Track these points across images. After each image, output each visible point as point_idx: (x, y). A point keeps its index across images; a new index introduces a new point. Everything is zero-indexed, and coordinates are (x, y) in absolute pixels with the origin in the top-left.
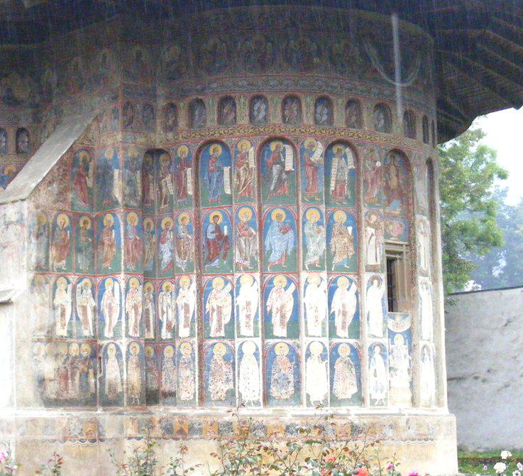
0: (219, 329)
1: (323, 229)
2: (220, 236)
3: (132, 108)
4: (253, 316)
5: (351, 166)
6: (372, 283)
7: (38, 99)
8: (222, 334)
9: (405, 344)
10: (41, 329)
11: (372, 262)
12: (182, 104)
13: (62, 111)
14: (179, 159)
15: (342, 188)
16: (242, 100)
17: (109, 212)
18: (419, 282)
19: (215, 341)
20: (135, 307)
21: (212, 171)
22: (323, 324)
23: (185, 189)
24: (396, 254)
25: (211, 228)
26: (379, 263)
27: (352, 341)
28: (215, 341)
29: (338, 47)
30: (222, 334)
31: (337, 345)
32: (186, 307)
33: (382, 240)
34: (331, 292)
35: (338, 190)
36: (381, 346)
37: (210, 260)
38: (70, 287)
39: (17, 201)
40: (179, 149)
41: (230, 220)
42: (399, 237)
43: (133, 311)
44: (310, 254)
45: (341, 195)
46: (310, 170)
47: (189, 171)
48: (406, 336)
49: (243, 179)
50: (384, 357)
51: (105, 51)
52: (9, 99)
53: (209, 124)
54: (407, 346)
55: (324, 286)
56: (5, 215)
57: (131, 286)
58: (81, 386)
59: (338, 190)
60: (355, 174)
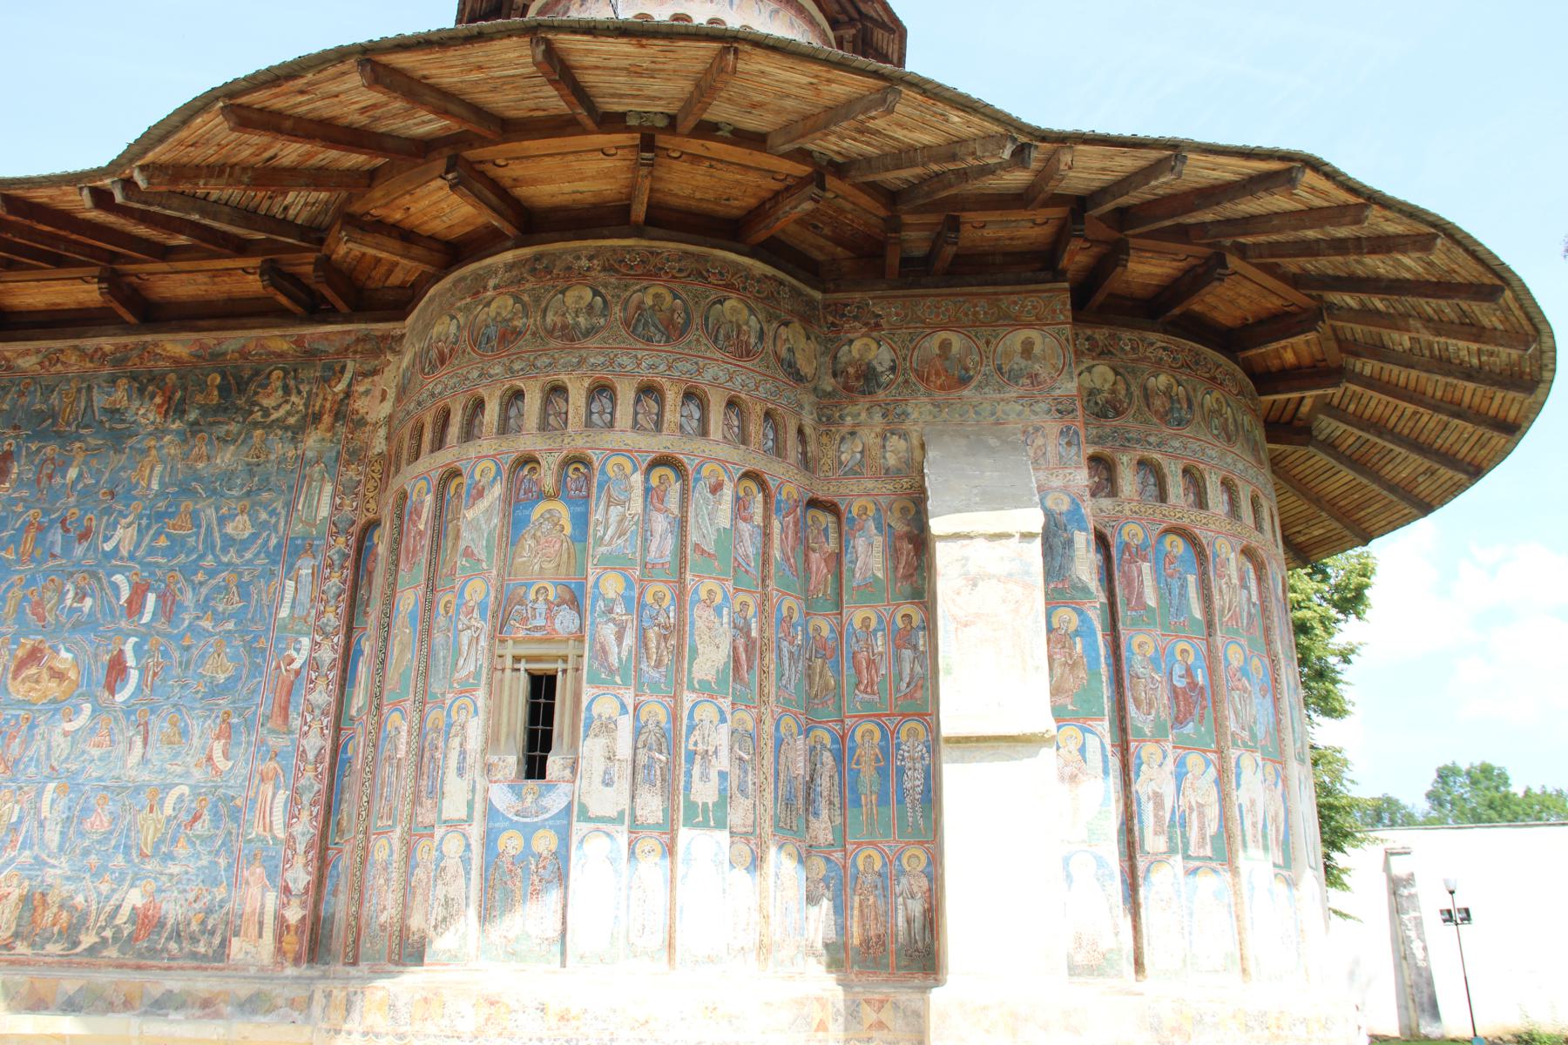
0: (1202, 845)
2: (1193, 685)
4: (1260, 826)
7: (828, 384)
8: (1208, 852)
12: (1125, 459)
13: (905, 414)
14: (1127, 545)
16: (1214, 477)
17: (1066, 605)
19: (1197, 863)
21: (1171, 576)
23: (1140, 595)
25: (1178, 670)
28: (1197, 863)
30: (1208, 852)
32: (1158, 798)
37: (1179, 721)
39: (1008, 536)
40: (1126, 529)
41: (1212, 661)
47: (1146, 567)
49: (1227, 599)
51: (1033, 334)
52: (790, 365)
53: (1172, 499)
56: (967, 559)
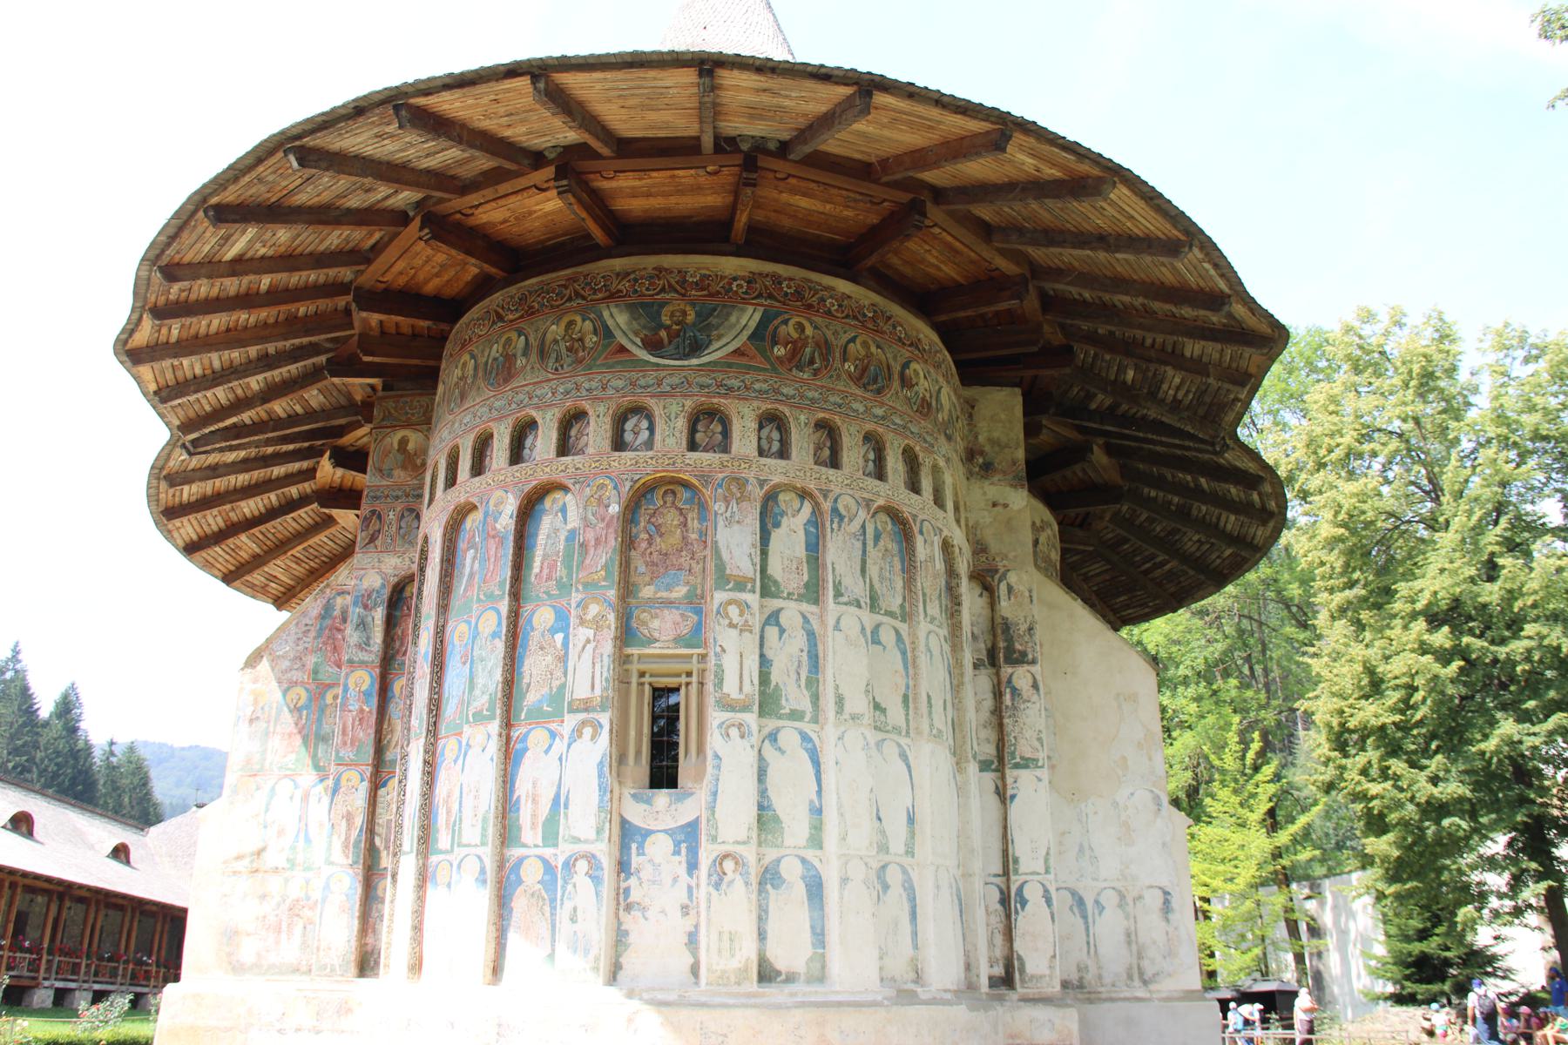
1: (500, 646)
3: (379, 517)
5: (574, 520)
6: (580, 736)
9: (677, 852)
10: (239, 858)
11: (581, 691)
15: (553, 567)
18: (715, 723)
20: (349, 817)
22: (485, 820)
24: (679, 675)
26: (598, 691)
27: (547, 852)
29: (556, 330)
31: (521, 860)
33: (608, 647)
34: (510, 756)
35: (546, 571)
36: (591, 858)
38: (299, 794)
42: (678, 640)
43: (344, 823)
44: (477, 692)
45: (549, 578)
46: (492, 544)
48: (681, 837)
50: (596, 880)
54: (683, 858)
55: (494, 746)
57: (343, 782)
58: (304, 945)
59: (546, 571)
60: (572, 534)
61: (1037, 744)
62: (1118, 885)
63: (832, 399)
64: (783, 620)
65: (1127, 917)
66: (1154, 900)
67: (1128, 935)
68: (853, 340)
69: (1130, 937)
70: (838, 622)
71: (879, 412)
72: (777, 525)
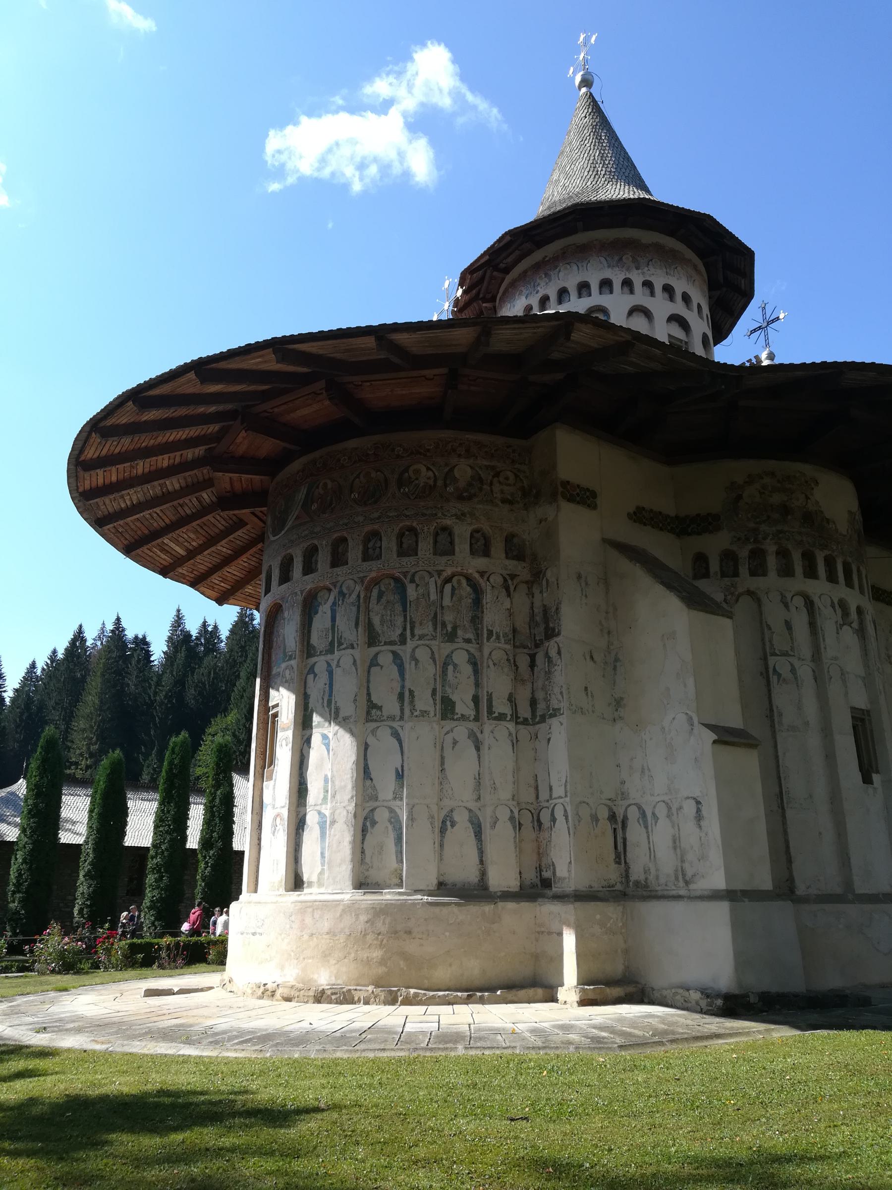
61: (560, 697)
62: (666, 798)
63: (341, 523)
64: (316, 670)
65: (673, 827)
66: (690, 808)
67: (674, 842)
68: (358, 477)
69: (676, 842)
70: (338, 662)
71: (376, 515)
72: (317, 613)
